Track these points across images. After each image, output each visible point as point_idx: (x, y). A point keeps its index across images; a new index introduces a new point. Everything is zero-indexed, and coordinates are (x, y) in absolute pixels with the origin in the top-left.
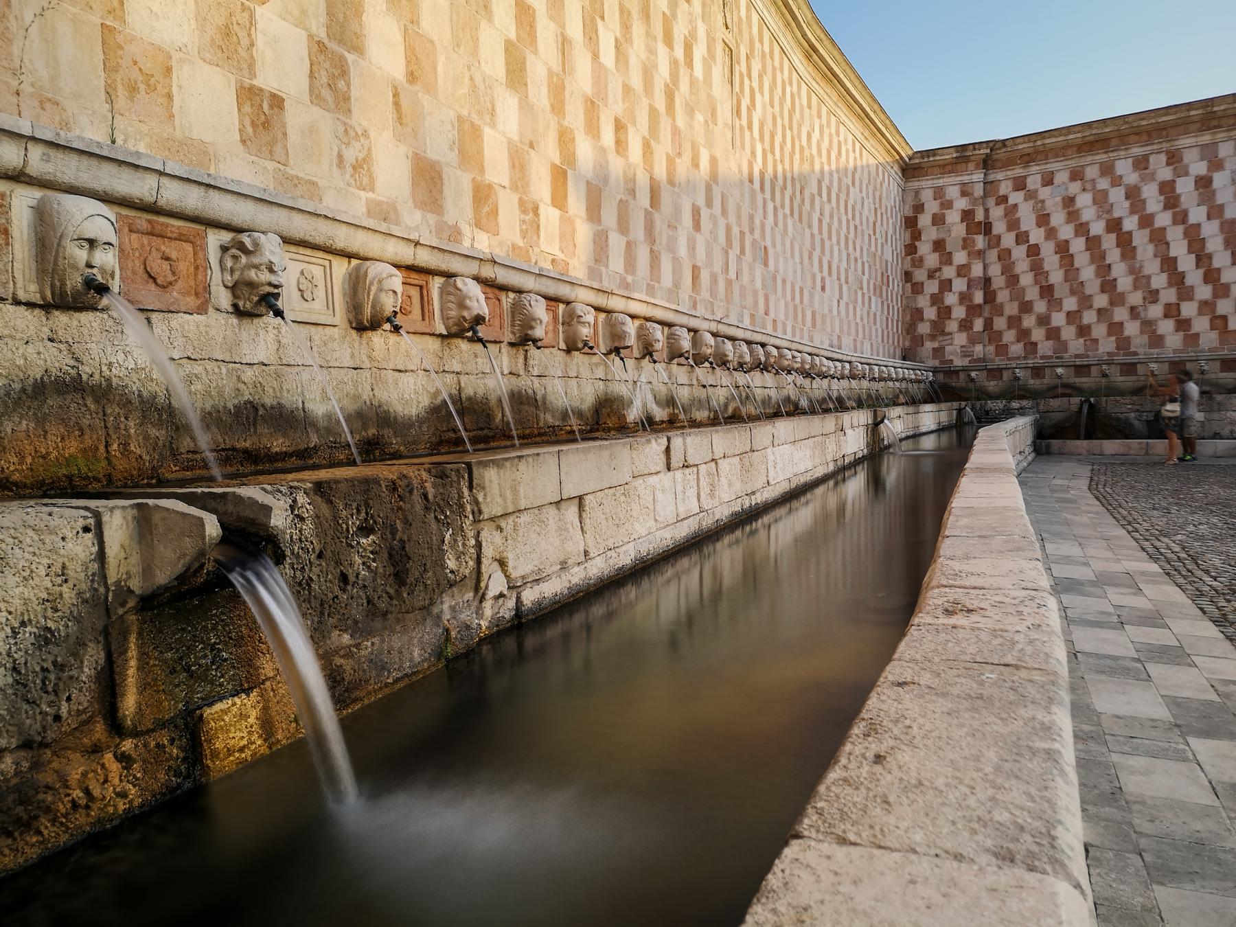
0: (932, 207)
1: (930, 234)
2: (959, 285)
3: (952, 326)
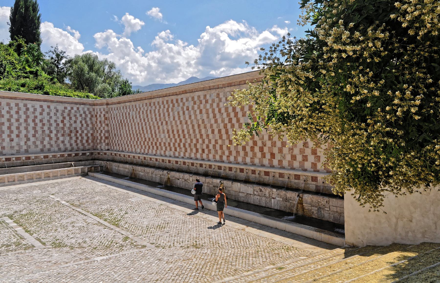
0: (99, 113)
1: (99, 119)
2: (103, 132)
3: (103, 141)
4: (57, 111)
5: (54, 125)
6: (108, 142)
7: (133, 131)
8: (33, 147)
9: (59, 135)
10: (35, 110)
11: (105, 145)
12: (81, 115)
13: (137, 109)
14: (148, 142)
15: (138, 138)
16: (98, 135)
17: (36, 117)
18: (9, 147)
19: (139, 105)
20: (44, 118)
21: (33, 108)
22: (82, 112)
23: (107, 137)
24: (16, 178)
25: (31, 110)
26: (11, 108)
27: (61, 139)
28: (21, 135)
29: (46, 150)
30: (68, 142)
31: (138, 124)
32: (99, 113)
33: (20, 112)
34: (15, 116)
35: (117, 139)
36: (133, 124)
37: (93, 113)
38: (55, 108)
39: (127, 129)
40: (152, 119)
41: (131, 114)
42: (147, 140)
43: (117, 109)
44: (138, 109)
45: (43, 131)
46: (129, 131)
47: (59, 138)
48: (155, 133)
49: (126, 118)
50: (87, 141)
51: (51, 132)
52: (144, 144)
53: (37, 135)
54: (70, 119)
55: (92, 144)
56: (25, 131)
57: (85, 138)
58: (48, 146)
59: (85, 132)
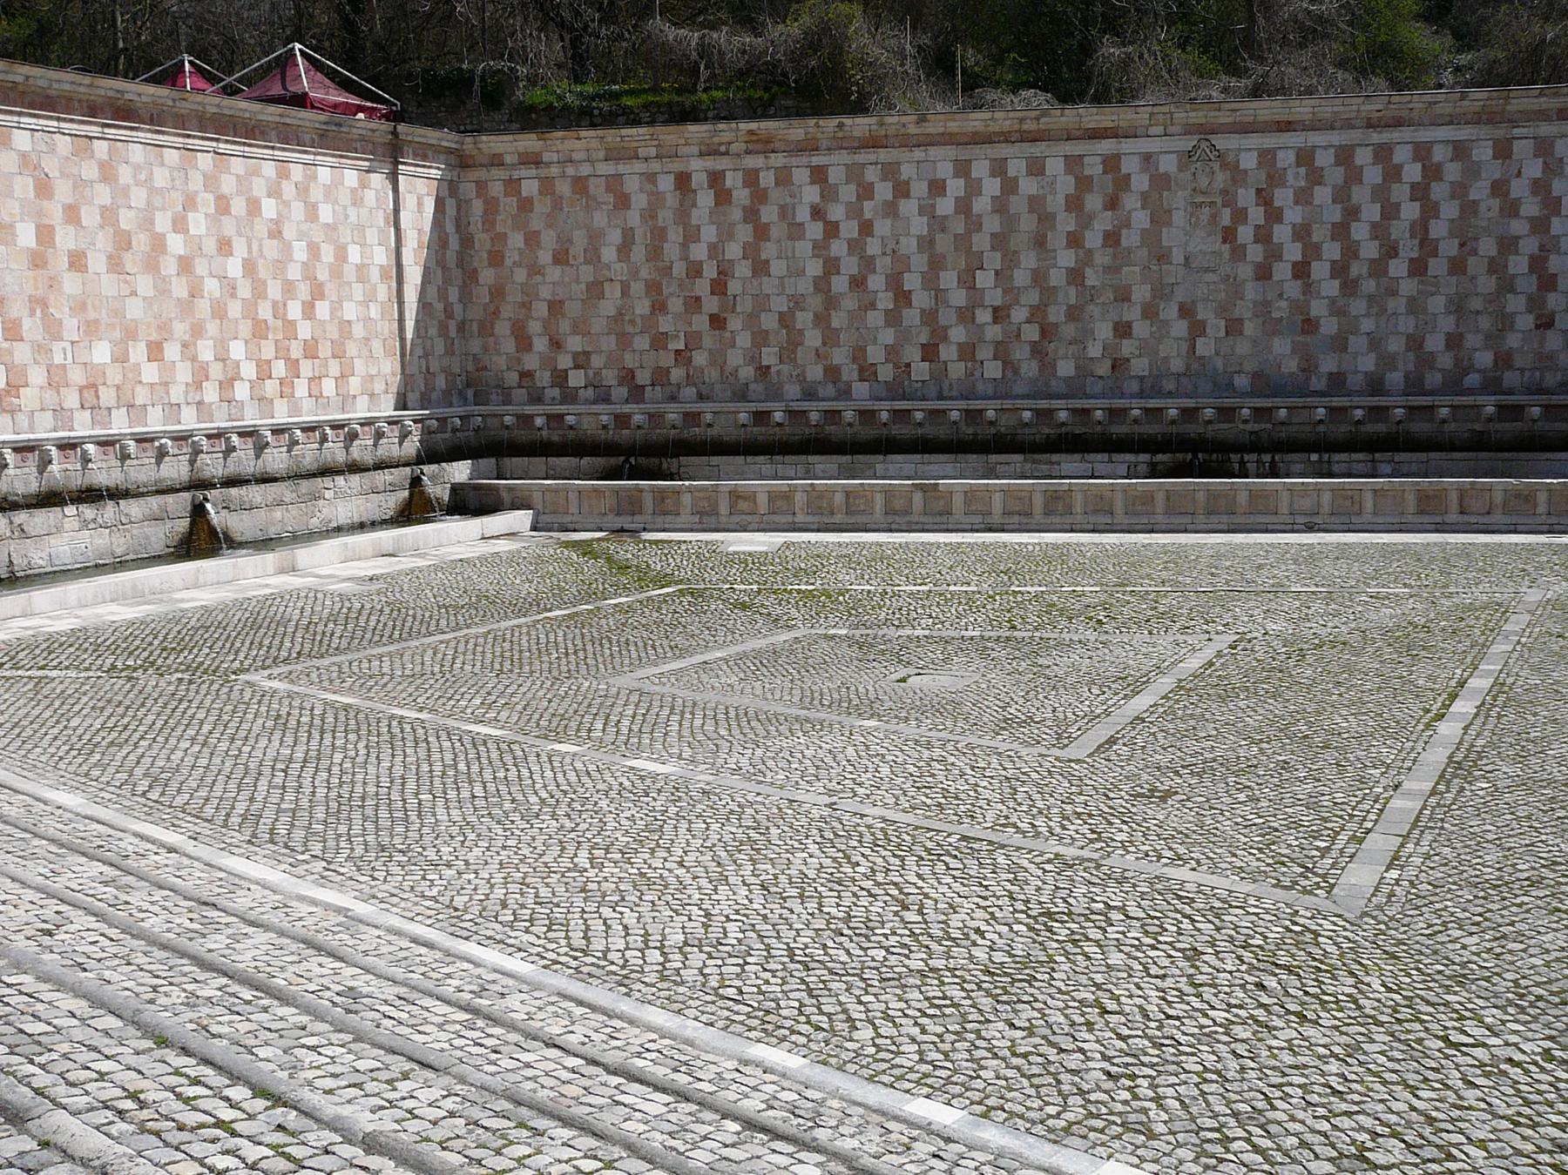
24: (1498, 498)
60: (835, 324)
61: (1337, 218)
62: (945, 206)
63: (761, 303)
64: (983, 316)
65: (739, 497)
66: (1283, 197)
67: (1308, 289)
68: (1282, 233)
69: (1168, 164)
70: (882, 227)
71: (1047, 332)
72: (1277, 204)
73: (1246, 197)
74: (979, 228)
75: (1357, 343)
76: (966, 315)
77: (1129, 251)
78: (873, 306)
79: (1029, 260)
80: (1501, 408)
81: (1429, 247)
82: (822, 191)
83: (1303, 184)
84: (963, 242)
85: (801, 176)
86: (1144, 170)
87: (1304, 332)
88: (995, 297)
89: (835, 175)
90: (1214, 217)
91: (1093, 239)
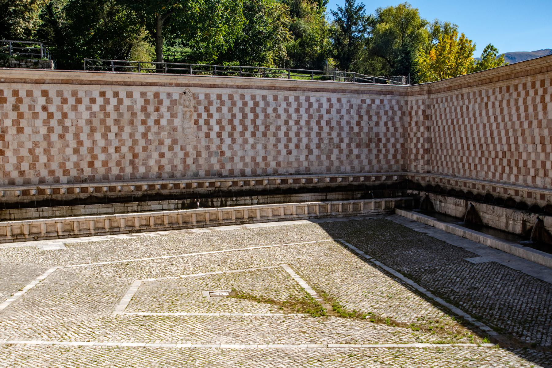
0: (415, 108)
1: (414, 119)
2: (421, 140)
3: (420, 157)
4: (351, 106)
5: (346, 129)
6: (429, 158)
7: (473, 139)
8: (316, 163)
9: (353, 145)
10: (321, 105)
11: (424, 163)
12: (386, 113)
13: (482, 99)
14: (501, 160)
15: (483, 153)
16: (412, 146)
17: (321, 117)
18: (286, 164)
19: (487, 91)
20: (333, 119)
21: (318, 103)
22: (387, 107)
23: (427, 149)
25: (315, 106)
26: (289, 105)
27: (356, 151)
28: (301, 145)
29: (333, 168)
30: (365, 157)
31: (484, 126)
32: (415, 108)
33: (301, 109)
34: (294, 116)
35: (445, 153)
36: (475, 126)
37: (404, 109)
38: (347, 102)
39: (463, 135)
40: (510, 116)
41: (470, 109)
42: (500, 155)
43: (446, 101)
44: (485, 100)
45: (331, 139)
46: (467, 139)
47: (352, 150)
48: (516, 143)
49: (462, 116)
50: (395, 156)
51: (341, 140)
52: (494, 163)
53: (322, 146)
54: (369, 120)
55: (401, 162)
56: (307, 138)
57: (392, 151)
58: (336, 164)
59: (392, 140)
60: (52, 153)
61: (230, 117)
62: (96, 108)
63: (21, 144)
64: (111, 150)
65: (33, 227)
66: (213, 109)
67: (222, 141)
68: (213, 122)
69: (176, 97)
70: (72, 115)
71: (135, 156)
72: (211, 112)
73: (201, 109)
74: (109, 117)
75: (237, 159)
76: (105, 150)
77: (163, 126)
78: (68, 146)
79: (128, 129)
80: (282, 180)
81: (256, 128)
82: (46, 100)
83: (219, 105)
84: (103, 122)
85: (37, 93)
86: (168, 98)
87: (221, 156)
88: (116, 143)
89: (52, 94)
90: (191, 115)
91: (151, 122)
